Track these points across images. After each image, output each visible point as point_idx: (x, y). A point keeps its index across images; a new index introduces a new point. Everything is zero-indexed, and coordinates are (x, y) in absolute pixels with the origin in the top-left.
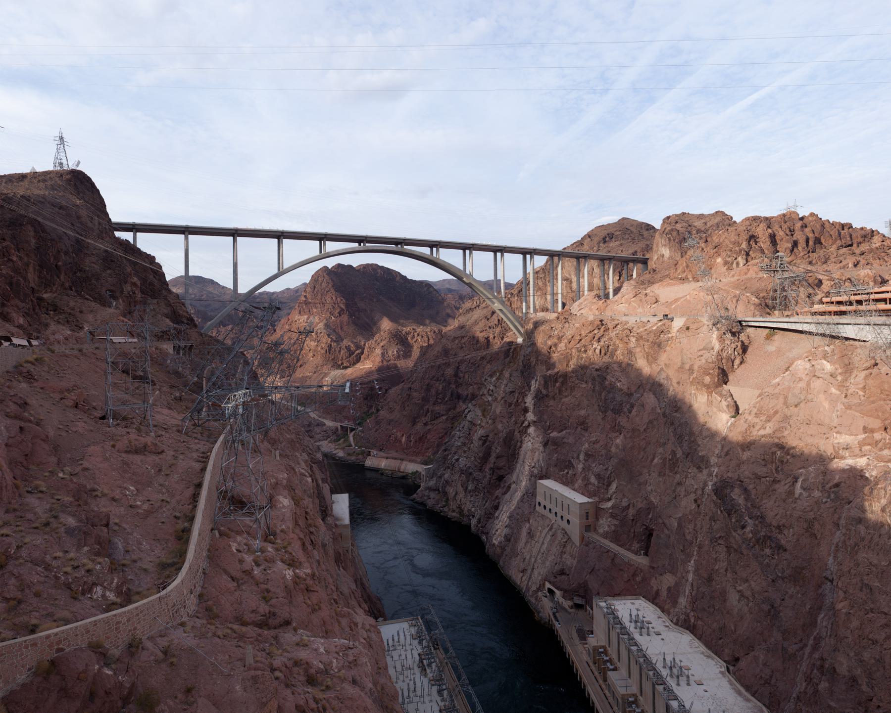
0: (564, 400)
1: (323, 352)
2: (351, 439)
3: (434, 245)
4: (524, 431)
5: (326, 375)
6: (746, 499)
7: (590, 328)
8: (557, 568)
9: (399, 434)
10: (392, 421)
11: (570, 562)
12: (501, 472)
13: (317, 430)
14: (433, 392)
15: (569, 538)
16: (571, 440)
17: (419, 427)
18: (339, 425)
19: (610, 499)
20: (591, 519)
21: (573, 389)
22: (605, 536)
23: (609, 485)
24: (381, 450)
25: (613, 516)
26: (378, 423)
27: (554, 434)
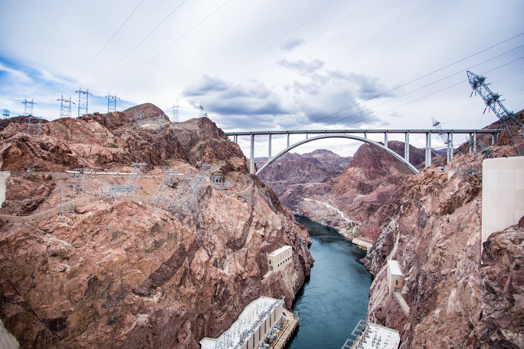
0: (408, 217)
1: (357, 186)
2: (354, 229)
3: (365, 132)
4: (396, 234)
5: (355, 197)
6: (422, 284)
7: (426, 177)
8: (380, 306)
9: (374, 230)
10: (372, 222)
11: (384, 305)
12: (384, 254)
13: (342, 223)
14: (392, 208)
15: (388, 293)
16: (406, 241)
17: (381, 227)
18: (351, 221)
19: (408, 276)
20: (399, 285)
21: (412, 211)
22: (403, 296)
23: (410, 268)
24: (363, 236)
25: (408, 286)
26: (367, 223)
27: (403, 236)
